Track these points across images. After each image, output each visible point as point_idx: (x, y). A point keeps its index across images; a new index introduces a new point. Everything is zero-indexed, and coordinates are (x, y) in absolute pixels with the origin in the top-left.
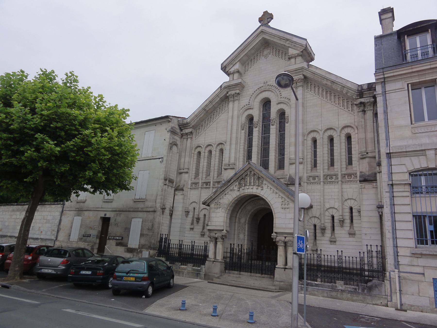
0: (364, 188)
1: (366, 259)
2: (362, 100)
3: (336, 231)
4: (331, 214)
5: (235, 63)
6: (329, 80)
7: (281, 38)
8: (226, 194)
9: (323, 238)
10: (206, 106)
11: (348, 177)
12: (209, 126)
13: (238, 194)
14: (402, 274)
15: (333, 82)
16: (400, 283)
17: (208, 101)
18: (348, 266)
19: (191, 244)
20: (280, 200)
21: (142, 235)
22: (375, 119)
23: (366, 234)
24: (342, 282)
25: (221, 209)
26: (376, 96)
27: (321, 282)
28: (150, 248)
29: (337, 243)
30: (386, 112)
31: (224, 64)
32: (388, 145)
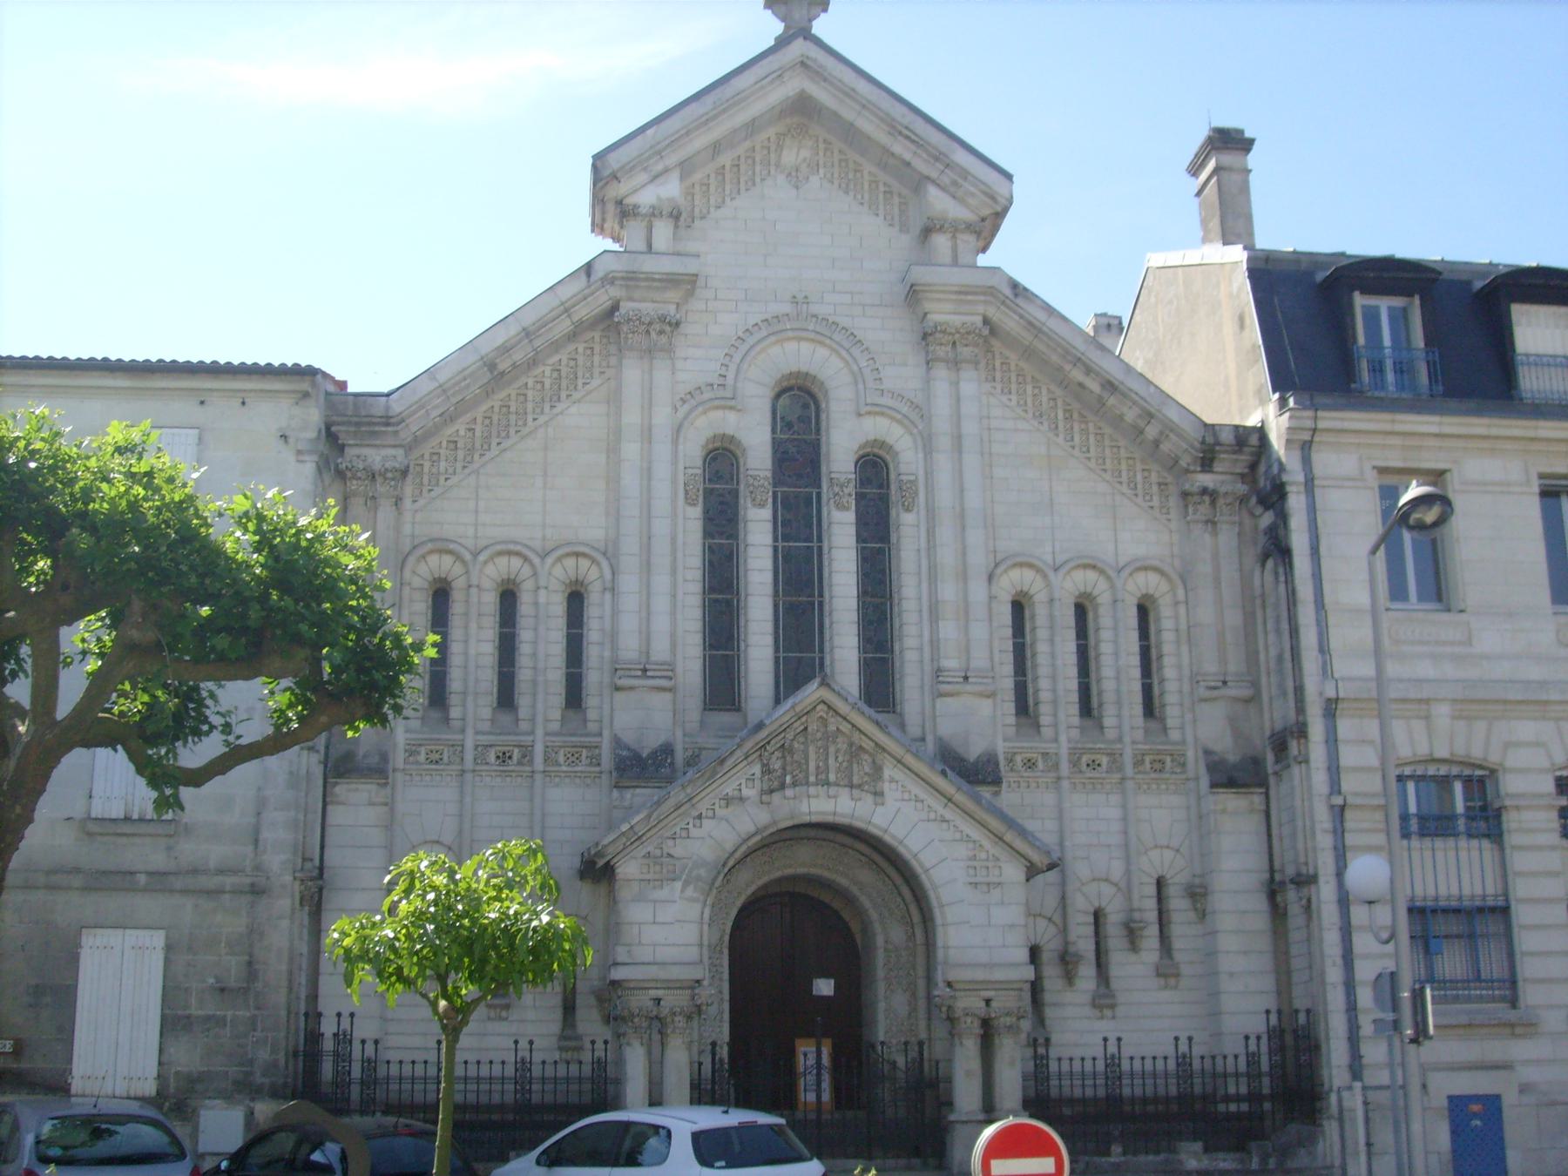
0: (1224, 811)
1: (1265, 1060)
2: (1206, 480)
3: (1114, 971)
4: (1103, 904)
5: (660, 167)
6: (1097, 374)
7: (895, 129)
8: (700, 817)
9: (1069, 996)
10: (505, 349)
11: (1160, 764)
12: (495, 450)
13: (763, 817)
14: (1371, 1095)
15: (1110, 386)
16: (1367, 1120)
17: (513, 329)
18: (1066, 1091)
19: (1241, 1050)
20: (962, 851)
21: (173, 1024)
22: (1281, 570)
23: (1231, 975)
24: (1198, 1146)
25: (678, 885)
26: (1288, 488)
27: (1124, 1154)
28: (244, 1088)
29: (1120, 1011)
30: (1315, 551)
31: (614, 161)
32: (1326, 671)
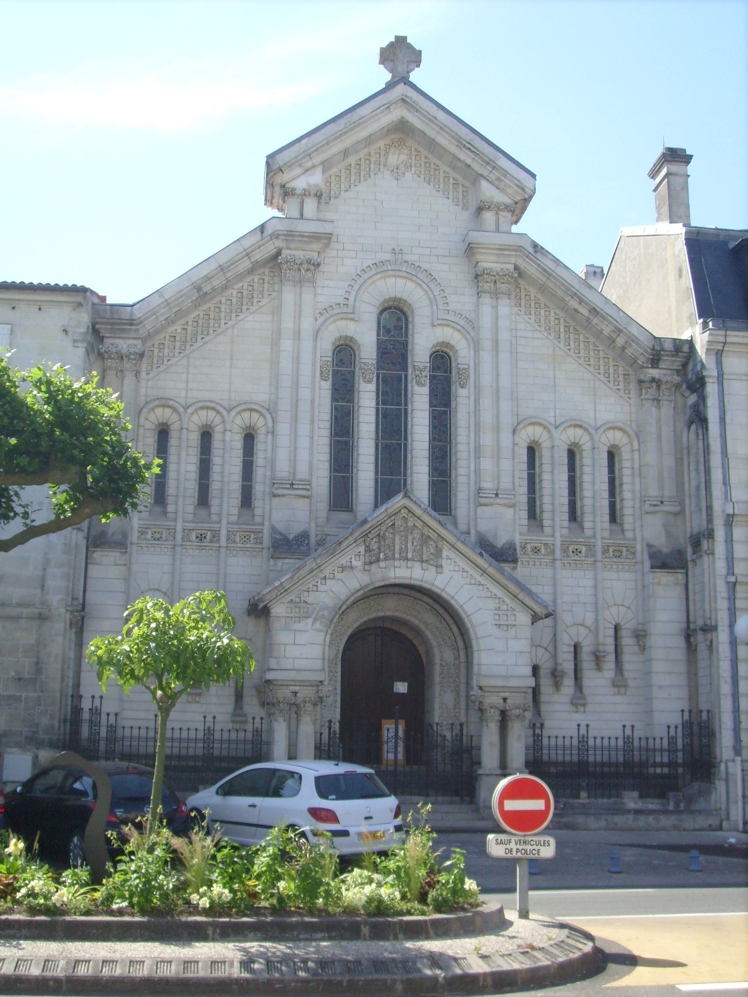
0: (659, 584)
2: (654, 373)
3: (586, 682)
4: (580, 640)
5: (309, 164)
6: (587, 304)
7: (461, 144)
8: (325, 578)
9: (556, 698)
10: (208, 278)
11: (619, 553)
12: (199, 343)
13: (365, 579)
15: (594, 311)
17: (213, 266)
18: (553, 758)
19: (665, 735)
20: (492, 604)
22: (700, 432)
23: (660, 687)
24: (635, 794)
25: (310, 620)
26: (707, 380)
28: (32, 741)
29: (589, 708)
31: (280, 160)
32: (727, 497)
